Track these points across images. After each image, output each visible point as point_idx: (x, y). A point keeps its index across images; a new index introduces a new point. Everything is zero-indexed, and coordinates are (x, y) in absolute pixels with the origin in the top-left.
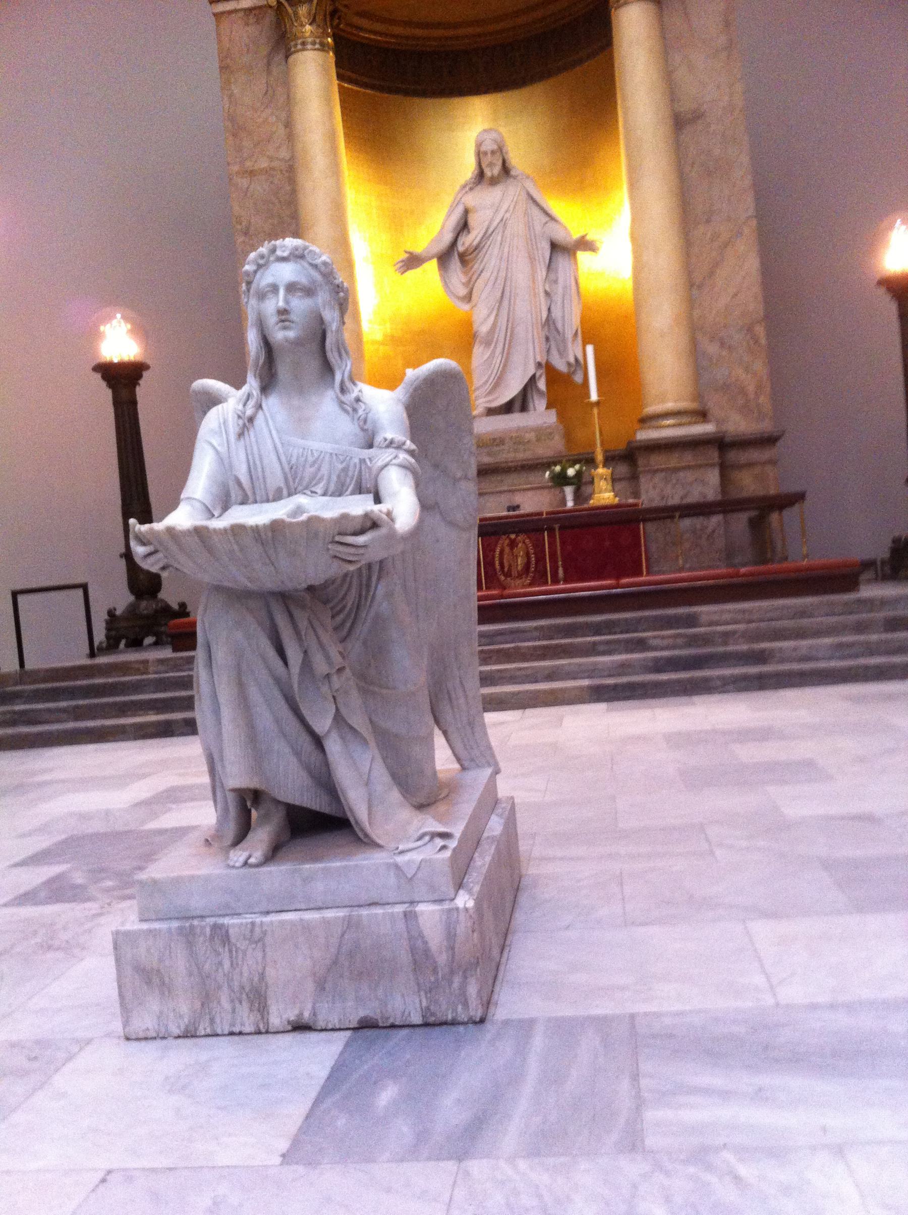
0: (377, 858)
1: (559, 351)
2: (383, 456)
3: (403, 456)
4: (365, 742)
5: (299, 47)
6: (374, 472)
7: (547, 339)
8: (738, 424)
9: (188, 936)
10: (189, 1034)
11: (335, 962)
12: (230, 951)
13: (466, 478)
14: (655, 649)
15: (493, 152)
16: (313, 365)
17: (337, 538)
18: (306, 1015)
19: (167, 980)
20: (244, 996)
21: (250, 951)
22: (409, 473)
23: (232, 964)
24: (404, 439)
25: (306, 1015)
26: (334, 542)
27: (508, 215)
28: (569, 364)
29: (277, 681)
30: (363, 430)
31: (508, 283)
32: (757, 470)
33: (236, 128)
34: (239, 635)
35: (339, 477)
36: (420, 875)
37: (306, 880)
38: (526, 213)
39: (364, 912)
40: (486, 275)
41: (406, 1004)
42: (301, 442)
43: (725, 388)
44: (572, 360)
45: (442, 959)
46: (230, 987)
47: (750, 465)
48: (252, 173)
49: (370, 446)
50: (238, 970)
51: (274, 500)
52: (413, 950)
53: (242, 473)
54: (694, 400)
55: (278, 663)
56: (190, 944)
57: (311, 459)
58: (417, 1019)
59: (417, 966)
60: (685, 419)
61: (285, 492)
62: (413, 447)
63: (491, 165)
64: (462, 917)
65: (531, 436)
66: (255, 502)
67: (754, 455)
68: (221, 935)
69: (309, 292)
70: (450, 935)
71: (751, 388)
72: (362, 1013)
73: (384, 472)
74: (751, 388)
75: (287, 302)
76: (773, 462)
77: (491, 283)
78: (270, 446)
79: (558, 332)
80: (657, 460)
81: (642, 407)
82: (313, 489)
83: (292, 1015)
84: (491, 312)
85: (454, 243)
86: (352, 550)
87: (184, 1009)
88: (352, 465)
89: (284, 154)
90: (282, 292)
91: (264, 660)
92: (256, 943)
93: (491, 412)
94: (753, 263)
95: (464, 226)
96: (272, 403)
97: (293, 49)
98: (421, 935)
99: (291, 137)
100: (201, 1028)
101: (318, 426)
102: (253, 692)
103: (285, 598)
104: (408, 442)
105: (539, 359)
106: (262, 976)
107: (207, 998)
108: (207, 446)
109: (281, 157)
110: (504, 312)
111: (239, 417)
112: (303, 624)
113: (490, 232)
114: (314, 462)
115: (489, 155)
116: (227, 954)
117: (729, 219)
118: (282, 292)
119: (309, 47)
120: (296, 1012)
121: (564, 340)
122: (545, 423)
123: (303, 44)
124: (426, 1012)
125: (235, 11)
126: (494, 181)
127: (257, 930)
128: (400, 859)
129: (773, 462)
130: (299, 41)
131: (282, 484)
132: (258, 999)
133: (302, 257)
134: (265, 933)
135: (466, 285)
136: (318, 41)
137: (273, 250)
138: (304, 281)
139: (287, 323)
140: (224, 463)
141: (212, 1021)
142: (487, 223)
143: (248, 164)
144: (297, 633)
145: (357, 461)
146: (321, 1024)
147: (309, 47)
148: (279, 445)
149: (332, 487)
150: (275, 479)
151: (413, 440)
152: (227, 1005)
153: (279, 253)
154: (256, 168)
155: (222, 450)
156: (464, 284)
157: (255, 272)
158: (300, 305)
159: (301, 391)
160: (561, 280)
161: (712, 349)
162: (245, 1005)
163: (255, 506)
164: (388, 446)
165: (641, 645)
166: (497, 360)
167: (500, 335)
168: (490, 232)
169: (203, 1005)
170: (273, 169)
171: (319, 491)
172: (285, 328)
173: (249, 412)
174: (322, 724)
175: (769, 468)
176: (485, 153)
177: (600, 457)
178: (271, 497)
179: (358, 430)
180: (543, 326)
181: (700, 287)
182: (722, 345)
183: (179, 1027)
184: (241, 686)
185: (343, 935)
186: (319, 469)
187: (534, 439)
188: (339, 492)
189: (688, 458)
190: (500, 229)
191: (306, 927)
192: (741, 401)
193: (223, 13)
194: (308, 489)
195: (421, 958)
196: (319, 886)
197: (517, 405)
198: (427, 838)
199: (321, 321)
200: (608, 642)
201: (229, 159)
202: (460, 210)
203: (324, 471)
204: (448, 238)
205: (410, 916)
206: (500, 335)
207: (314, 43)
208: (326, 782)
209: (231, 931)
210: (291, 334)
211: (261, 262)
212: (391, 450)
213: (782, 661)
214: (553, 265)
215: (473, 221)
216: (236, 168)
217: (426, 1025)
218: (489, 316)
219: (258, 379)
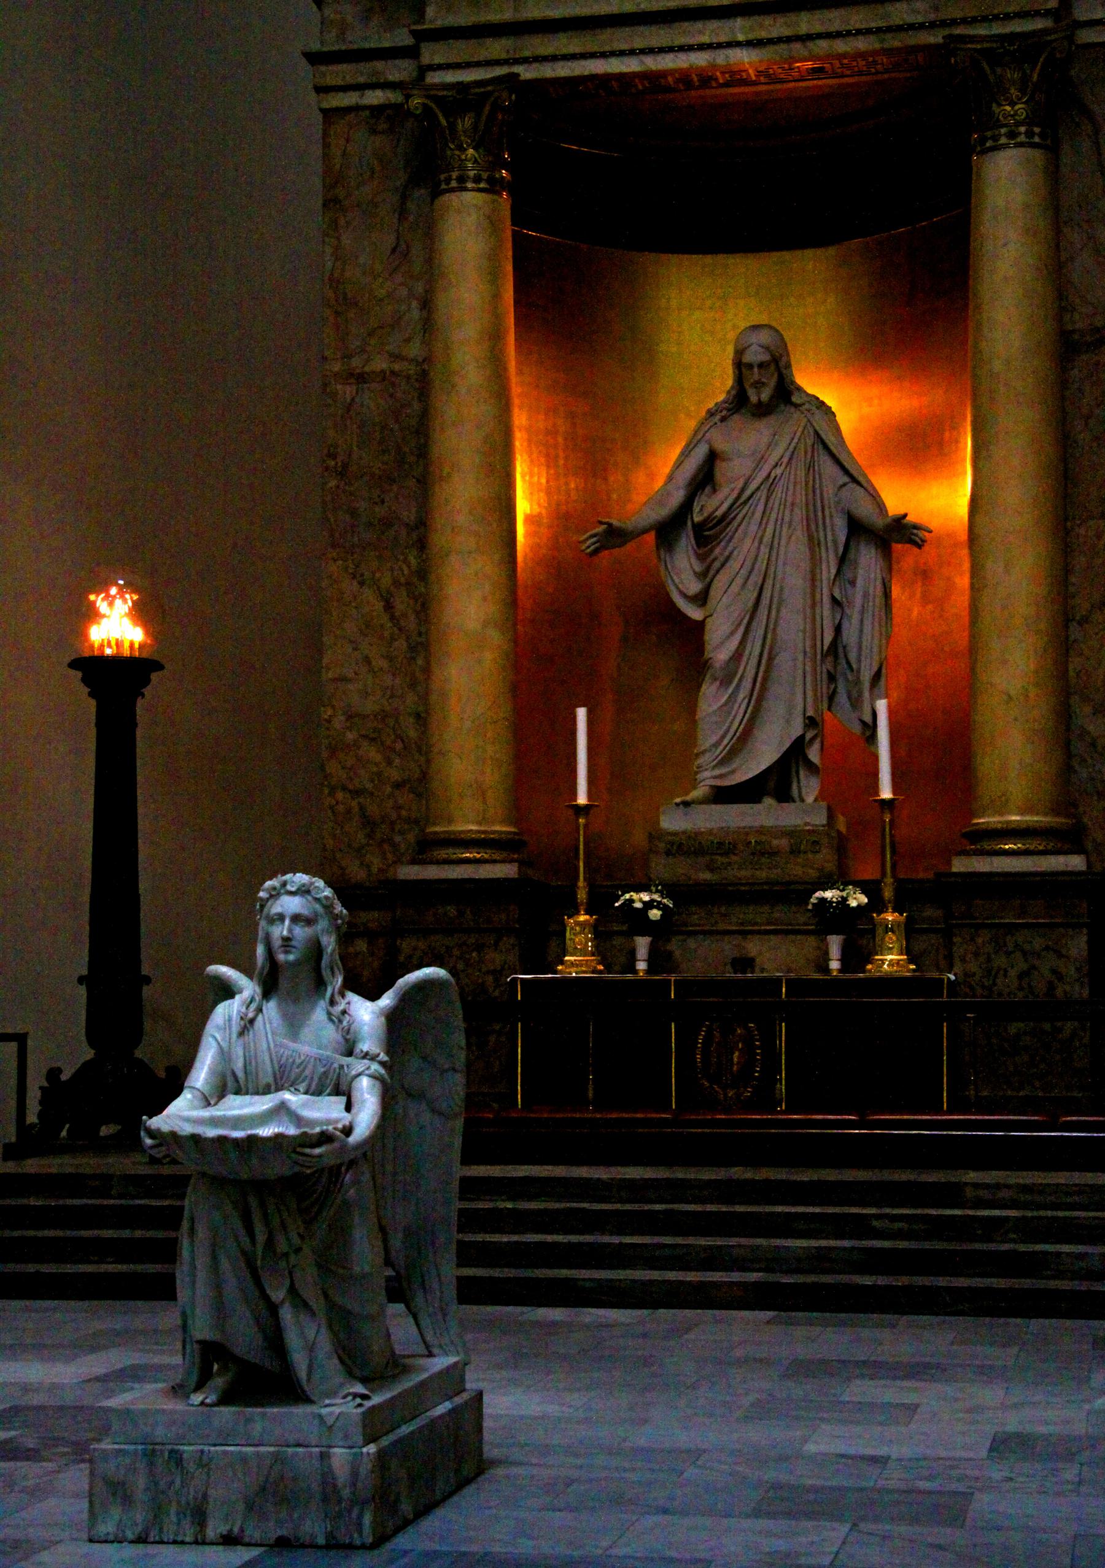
0: (310, 1409)
1: (849, 697)
2: (359, 1065)
3: (375, 1067)
4: (313, 1314)
5: (454, 184)
6: (349, 1079)
7: (832, 678)
10: (141, 1540)
11: (263, 1489)
13: (454, 1070)
15: (761, 365)
17: (298, 1149)
18: (236, 1530)
22: (377, 1083)
24: (378, 1051)
25: (236, 1530)
26: (295, 1151)
27: (778, 471)
29: (244, 1253)
30: (347, 1040)
31: (769, 582)
33: (343, 301)
34: (217, 1216)
35: (320, 1079)
36: (338, 1424)
38: (810, 467)
40: (734, 565)
41: (314, 1527)
42: (291, 1044)
45: (346, 1493)
48: (361, 378)
49: (350, 1053)
52: (324, 1483)
53: (239, 1065)
54: (1055, 811)
55: (246, 1240)
56: (151, 1464)
57: (298, 1061)
61: (273, 1087)
62: (386, 1058)
63: (759, 385)
64: (365, 1460)
65: (783, 843)
66: (247, 1093)
68: (177, 1458)
69: (309, 921)
70: (355, 1474)
72: (279, 1533)
73: (358, 1079)
75: (290, 930)
77: (739, 581)
78: (265, 1046)
79: (852, 670)
83: (223, 1529)
84: (736, 629)
85: (686, 507)
86: (309, 1159)
87: (139, 1517)
89: (415, 350)
90: (287, 922)
92: (203, 1466)
93: (722, 795)
95: (705, 479)
96: (271, 1008)
97: (443, 186)
99: (428, 325)
100: (152, 1535)
101: (306, 1033)
104: (382, 1054)
106: (205, 1496)
107: (158, 1511)
108: (211, 1039)
109: (412, 356)
110: (758, 631)
111: (242, 1018)
112: (271, 1208)
113: (748, 492)
115: (756, 370)
118: (287, 922)
119: (470, 185)
120: (228, 1527)
121: (858, 682)
122: (807, 824)
123: (462, 179)
124: (330, 1536)
125: (356, 108)
126: (762, 411)
127: (205, 1458)
128: (324, 1411)
130: (454, 175)
131: (270, 1080)
132: (199, 1515)
133: (308, 892)
134: (211, 1459)
135: (702, 576)
136: (485, 175)
137: (284, 884)
138: (305, 912)
140: (224, 1055)
141: (161, 1529)
142: (740, 484)
143: (356, 362)
144: (265, 1216)
145: (336, 1065)
147: (470, 185)
148: (272, 1045)
149: (313, 1087)
151: (387, 1053)
153: (289, 887)
154: (367, 369)
156: (695, 573)
157: (268, 899)
158: (301, 933)
159: (296, 1001)
160: (860, 582)
162: (189, 1518)
163: (248, 1097)
168: (748, 492)
170: (393, 372)
171: (302, 1090)
173: (251, 1015)
174: (278, 1295)
176: (750, 366)
178: (261, 1090)
179: (339, 1037)
180: (824, 656)
181: (1084, 621)
184: (214, 1258)
186: (304, 1071)
188: (318, 1093)
190: (763, 494)
191: (244, 1459)
193: (337, 110)
194: (292, 1085)
195: (329, 1490)
196: (258, 1427)
198: (350, 1398)
199: (319, 942)
201: (327, 353)
202: (701, 451)
204: (678, 497)
205: (324, 1457)
207: (477, 179)
208: (276, 1342)
209: (185, 1456)
210: (291, 957)
211: (273, 893)
212: (366, 1061)
213: (1060, 1275)
215: (722, 470)
216: (337, 367)
218: (732, 633)
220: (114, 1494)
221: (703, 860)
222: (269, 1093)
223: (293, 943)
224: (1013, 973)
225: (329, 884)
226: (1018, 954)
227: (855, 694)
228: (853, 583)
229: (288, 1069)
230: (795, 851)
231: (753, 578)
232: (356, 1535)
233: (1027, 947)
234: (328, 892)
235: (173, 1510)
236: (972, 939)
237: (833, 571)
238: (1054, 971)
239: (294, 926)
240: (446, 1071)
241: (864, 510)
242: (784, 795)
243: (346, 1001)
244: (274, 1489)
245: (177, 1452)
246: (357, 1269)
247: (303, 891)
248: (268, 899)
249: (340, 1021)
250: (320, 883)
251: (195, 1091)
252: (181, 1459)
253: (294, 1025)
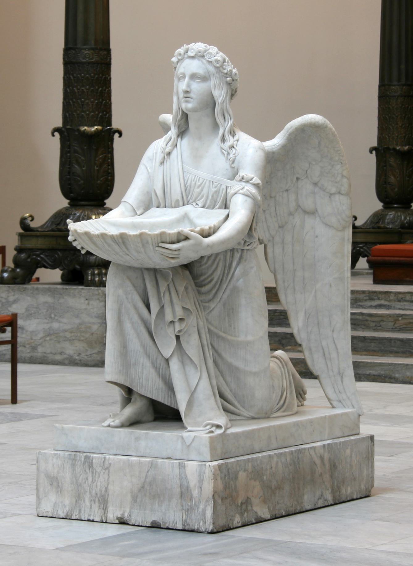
4: (196, 368)
9: (74, 461)
11: (143, 487)
12: (93, 472)
16: (207, 121)
17: (160, 245)
18: (126, 515)
19: (60, 484)
20: (97, 499)
21: (102, 473)
22: (249, 200)
23: (93, 481)
24: (252, 176)
26: (158, 246)
34: (120, 292)
35: (212, 196)
36: (193, 445)
37: (137, 439)
39: (160, 460)
41: (175, 517)
45: (195, 493)
46: (90, 493)
49: (233, 178)
50: (95, 484)
51: (175, 207)
52: (181, 486)
55: (144, 311)
56: (73, 465)
57: (198, 183)
58: (180, 527)
59: (182, 495)
61: (181, 203)
62: (259, 181)
68: (89, 463)
69: (204, 79)
75: (188, 85)
82: (197, 202)
87: (67, 502)
88: (221, 190)
90: (187, 79)
91: (136, 308)
92: (105, 469)
96: (185, 143)
98: (186, 478)
100: (74, 515)
102: (128, 326)
103: (155, 272)
106: (107, 489)
107: (78, 498)
116: (91, 474)
118: (187, 79)
120: (121, 513)
124: (185, 523)
127: (107, 463)
131: (180, 198)
132: (103, 501)
133: (203, 56)
138: (201, 72)
139: (187, 99)
146: (133, 522)
152: (88, 503)
158: (197, 87)
162: (97, 504)
164: (241, 181)
169: (76, 501)
172: (187, 102)
173: (168, 149)
178: (173, 206)
179: (228, 167)
183: (63, 512)
185: (148, 472)
186: (202, 190)
191: (131, 465)
196: (143, 443)
198: (208, 427)
203: (205, 191)
205: (182, 467)
209: (94, 461)
217: (184, 530)
219: (176, 128)
220: (51, 485)
222: (178, 206)
223: (192, 95)
225: (221, 49)
229: (192, 189)
232: (201, 523)
234: (220, 56)
235: (87, 497)
239: (192, 82)
240: (334, 194)
243: (236, 138)
244: (150, 489)
245: (89, 457)
246: (242, 338)
247: (200, 56)
248: (178, 62)
249: (228, 154)
250: (213, 50)
251: (127, 204)
252: (92, 463)
253: (197, 157)
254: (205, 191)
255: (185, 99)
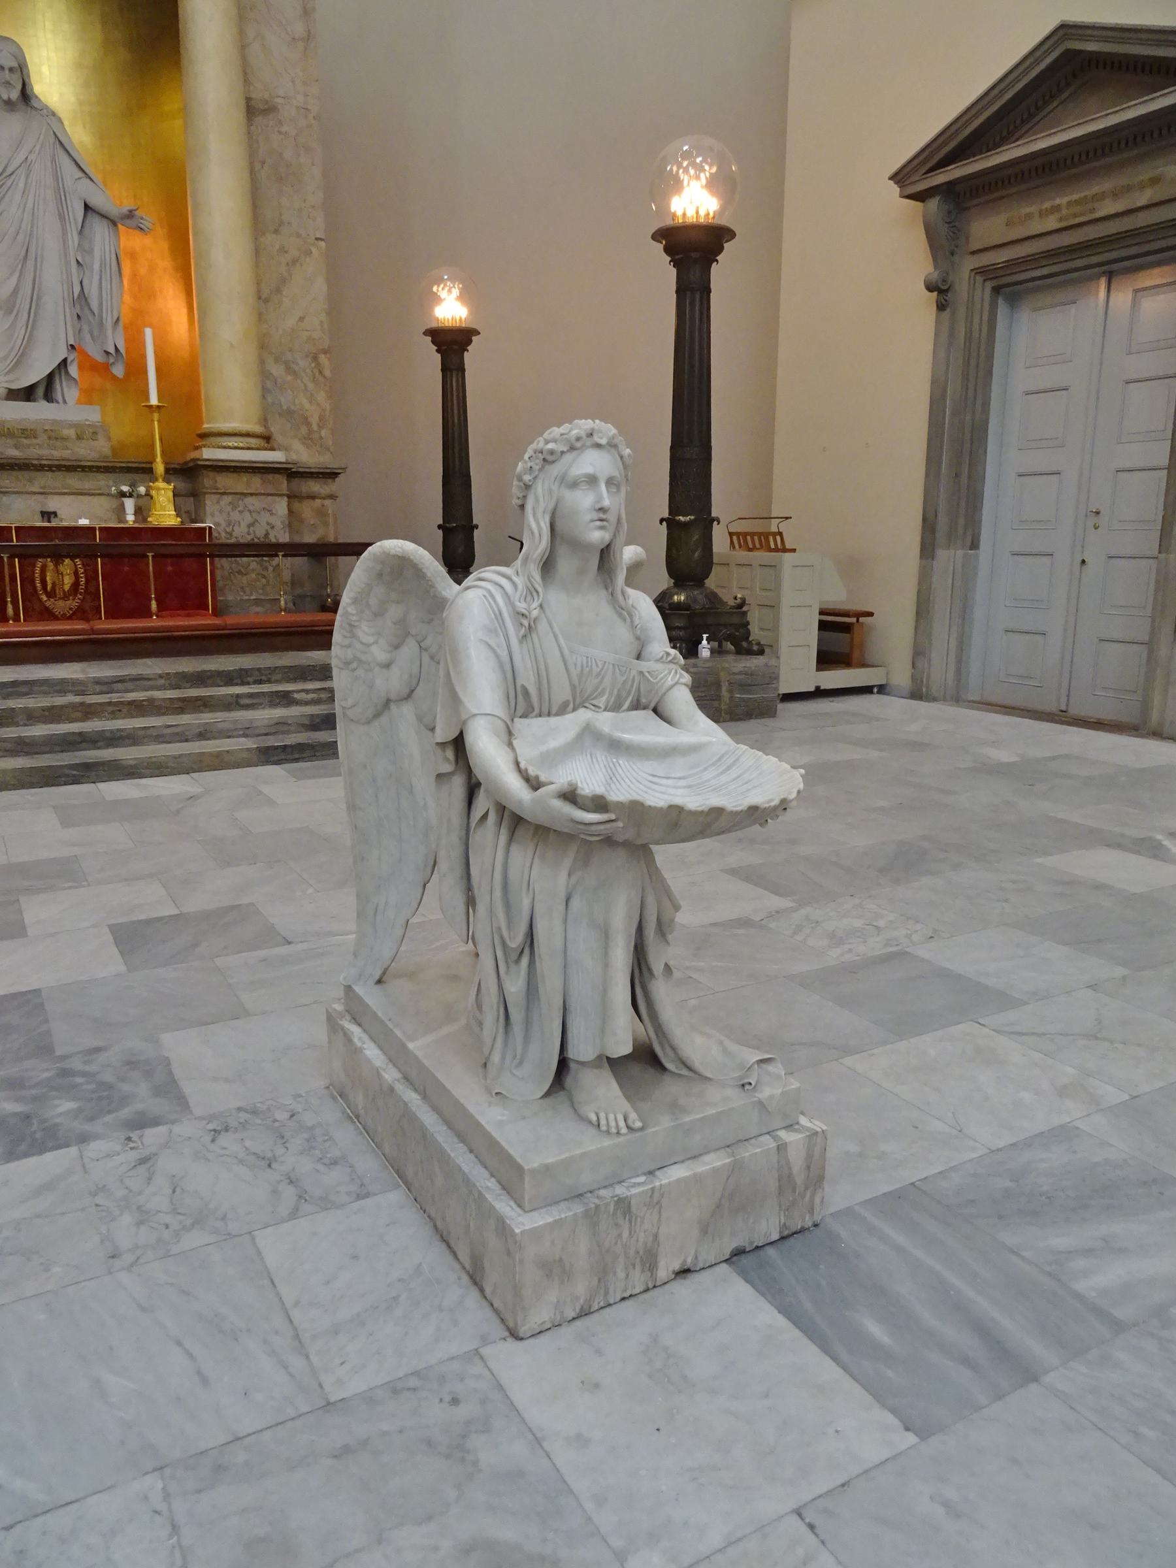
8: (303, 456)
12: (630, 1221)
14: (298, 703)
15: (11, 70)
20: (638, 1260)
25: (689, 1260)
27: (32, 157)
28: (107, 353)
32: (318, 502)
38: (53, 160)
43: (289, 414)
44: (112, 350)
45: (799, 1179)
47: (313, 497)
50: (635, 1238)
51: (557, 714)
57: (596, 670)
59: (781, 1191)
60: (253, 442)
61: (571, 706)
67: (314, 486)
71: (314, 420)
72: (734, 1245)
73: (670, 693)
74: (314, 420)
76: (332, 497)
80: (225, 481)
81: (201, 422)
82: (594, 702)
83: (677, 1266)
94: (320, 287)
98: (788, 1163)
105: (71, 342)
106: (656, 1236)
110: (29, 277)
114: (598, 674)
117: (299, 235)
121: (101, 324)
129: (332, 497)
150: (561, 692)
153: (596, 439)
155: (504, 654)
160: (97, 254)
161: (277, 370)
162: (638, 1267)
165: (285, 699)
166: (20, 332)
167: (23, 302)
169: (599, 1281)
175: (328, 502)
177: (160, 468)
181: (267, 301)
182: (288, 369)
183: (574, 1310)
186: (601, 682)
187: (74, 437)
188: (615, 707)
189: (256, 483)
192: (304, 430)
197: (40, 391)
200: (251, 696)
203: (608, 681)
206: (23, 302)
209: (633, 1201)
211: (578, 445)
214: (86, 231)
221: (10, 441)
224: (244, 525)
226: (247, 514)
227: (96, 333)
228: (90, 252)
230: (79, 438)
231: (21, 237)
233: (251, 508)
236: (218, 502)
237: (76, 242)
238: (268, 524)
241: (97, 201)
242: (49, 397)
254: (608, 681)
255: (598, 523)
